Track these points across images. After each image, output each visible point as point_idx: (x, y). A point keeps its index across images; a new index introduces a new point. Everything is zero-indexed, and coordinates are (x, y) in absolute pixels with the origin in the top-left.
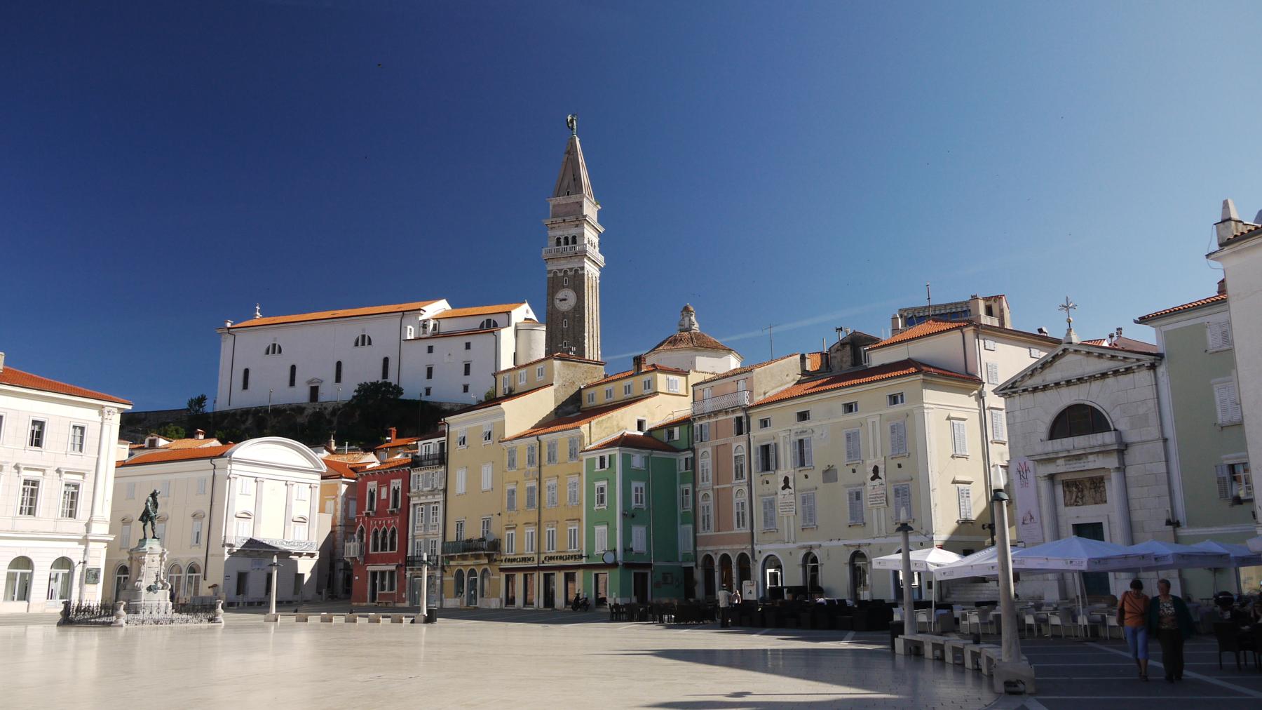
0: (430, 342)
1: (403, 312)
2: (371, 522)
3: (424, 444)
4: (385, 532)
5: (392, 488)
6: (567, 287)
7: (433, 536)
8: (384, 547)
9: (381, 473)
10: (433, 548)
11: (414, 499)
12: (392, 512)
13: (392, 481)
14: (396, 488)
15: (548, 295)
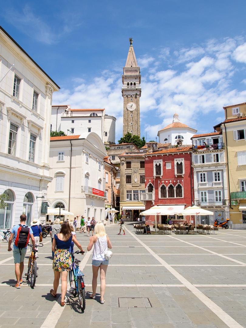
0: (73, 119)
1: (59, 106)
2: (159, 182)
3: (198, 139)
4: (171, 188)
5: (175, 163)
6: (132, 101)
7: (217, 189)
8: (171, 194)
9: (166, 155)
10: (218, 196)
11: (197, 169)
12: (180, 177)
13: (175, 159)
14: (179, 163)
15: (124, 104)
